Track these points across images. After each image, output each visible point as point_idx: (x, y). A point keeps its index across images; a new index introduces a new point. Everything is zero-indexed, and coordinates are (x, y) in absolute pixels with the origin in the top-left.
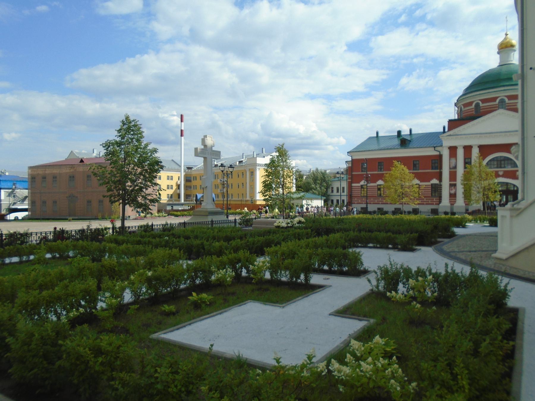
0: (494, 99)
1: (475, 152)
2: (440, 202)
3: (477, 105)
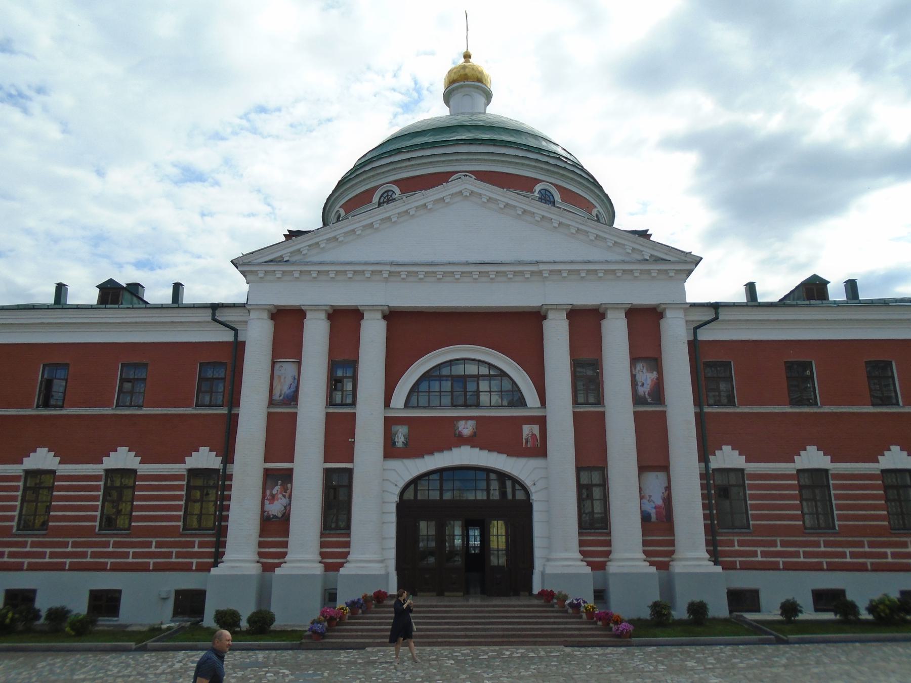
1: (373, 337)
2: (218, 557)
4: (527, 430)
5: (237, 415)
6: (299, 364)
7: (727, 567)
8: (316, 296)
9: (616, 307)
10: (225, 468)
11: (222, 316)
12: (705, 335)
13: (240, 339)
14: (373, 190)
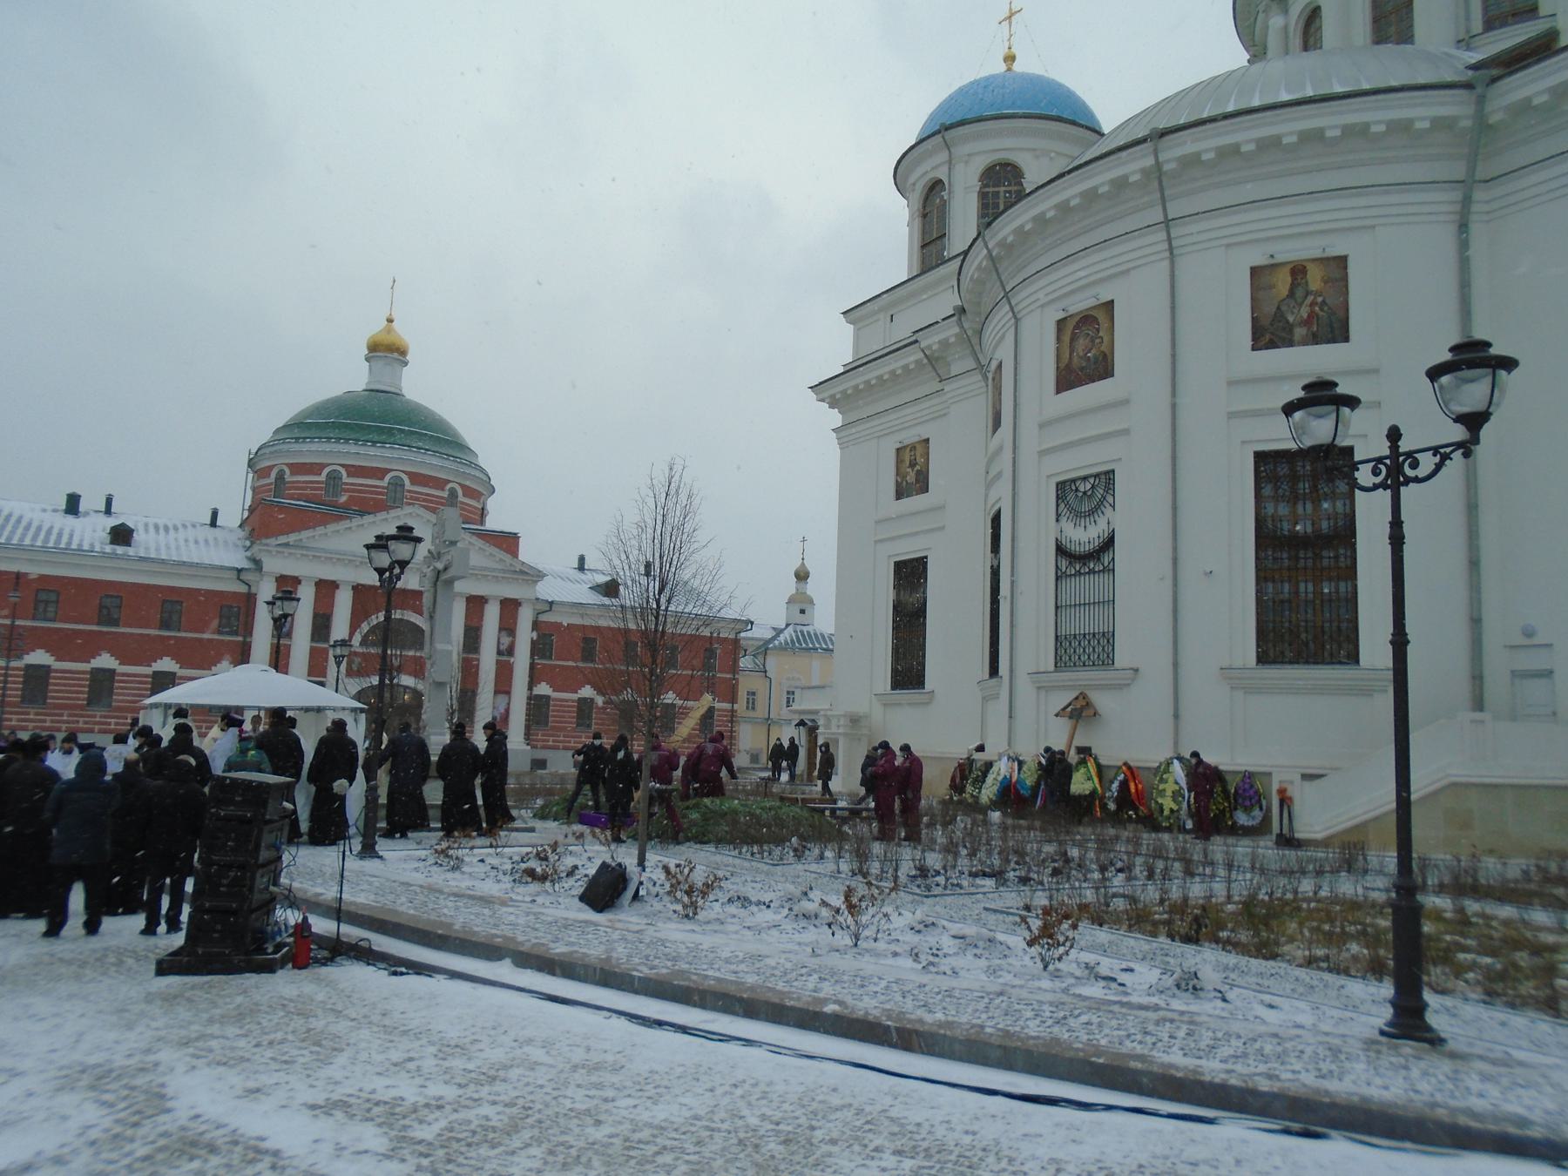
0: (380, 473)
3: (334, 477)
7: (534, 747)
8: (309, 571)
9: (495, 598)
11: (244, 576)
12: (544, 618)
13: (253, 590)
14: (323, 466)
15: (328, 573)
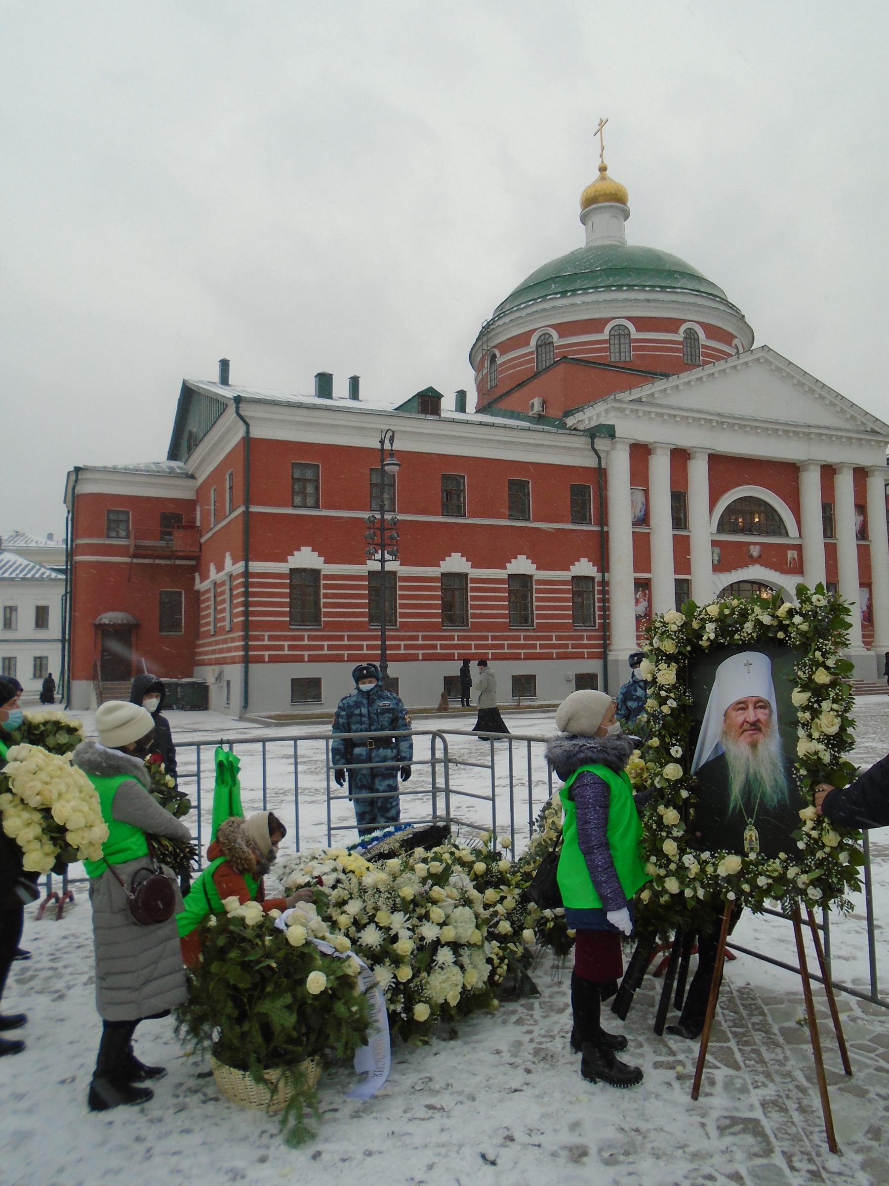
1: (699, 474)
4: (791, 554)
5: (607, 533)
6: (646, 493)
8: (662, 435)
10: (603, 576)
15: (684, 438)
